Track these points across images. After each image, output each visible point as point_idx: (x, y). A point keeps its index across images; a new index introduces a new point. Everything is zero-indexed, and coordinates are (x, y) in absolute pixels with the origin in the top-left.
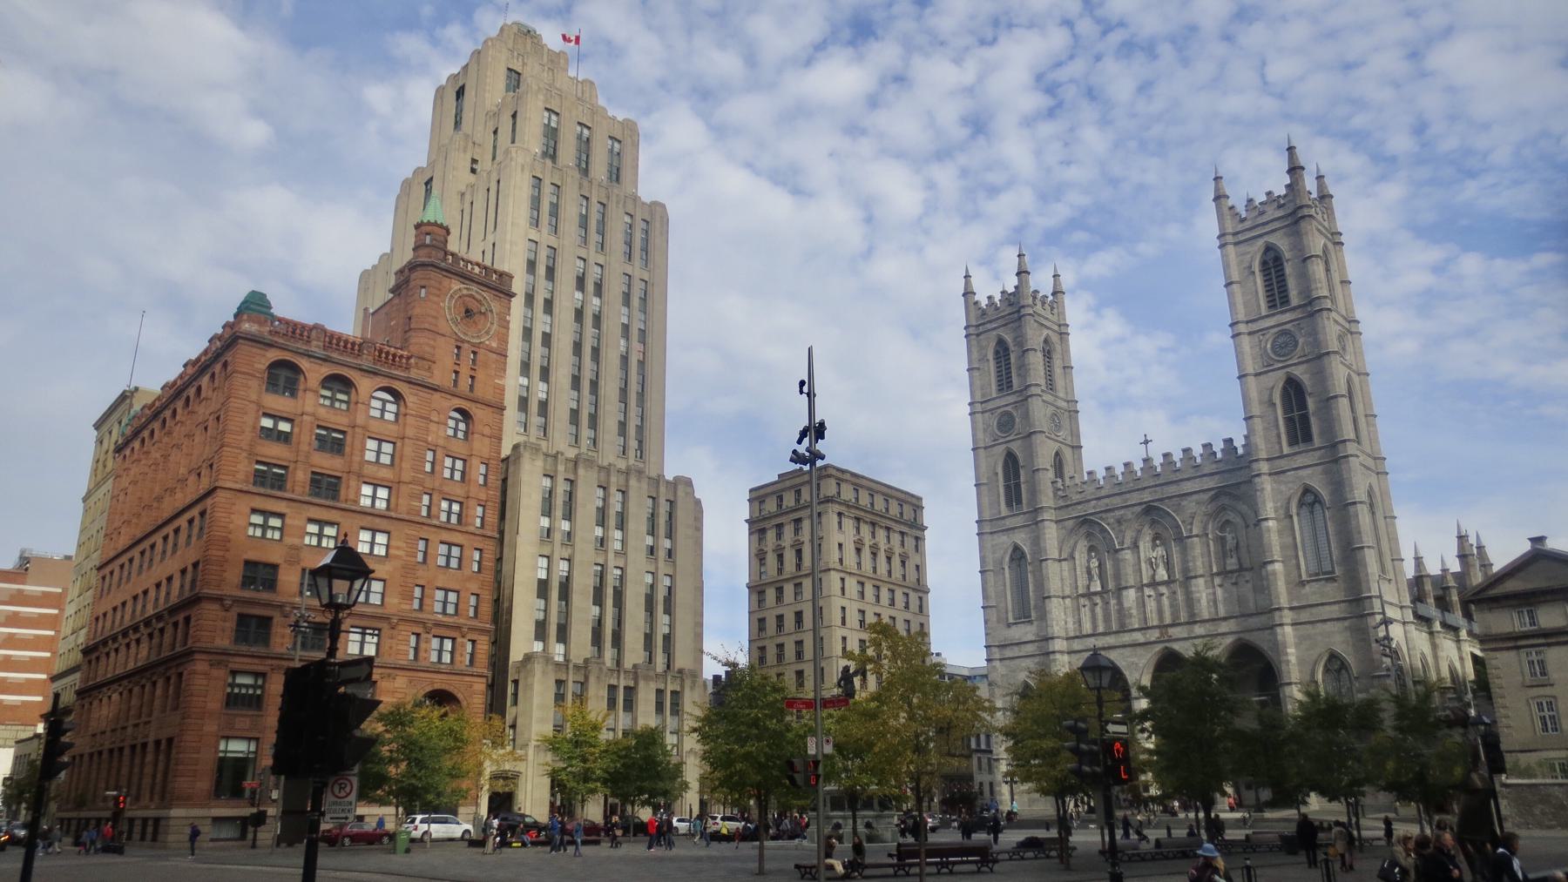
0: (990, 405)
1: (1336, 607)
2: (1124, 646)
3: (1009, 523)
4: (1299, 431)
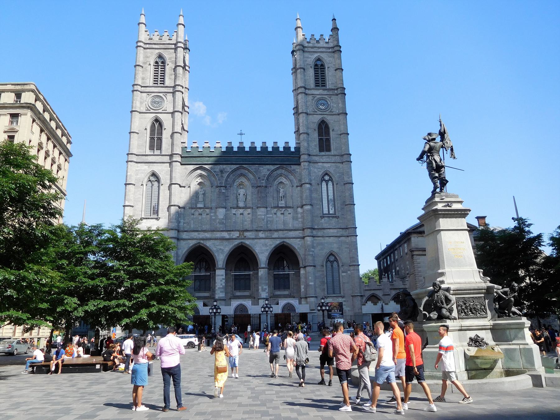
0: (148, 89)
1: (335, 231)
2: (216, 239)
3: (150, 159)
4: (325, 145)
